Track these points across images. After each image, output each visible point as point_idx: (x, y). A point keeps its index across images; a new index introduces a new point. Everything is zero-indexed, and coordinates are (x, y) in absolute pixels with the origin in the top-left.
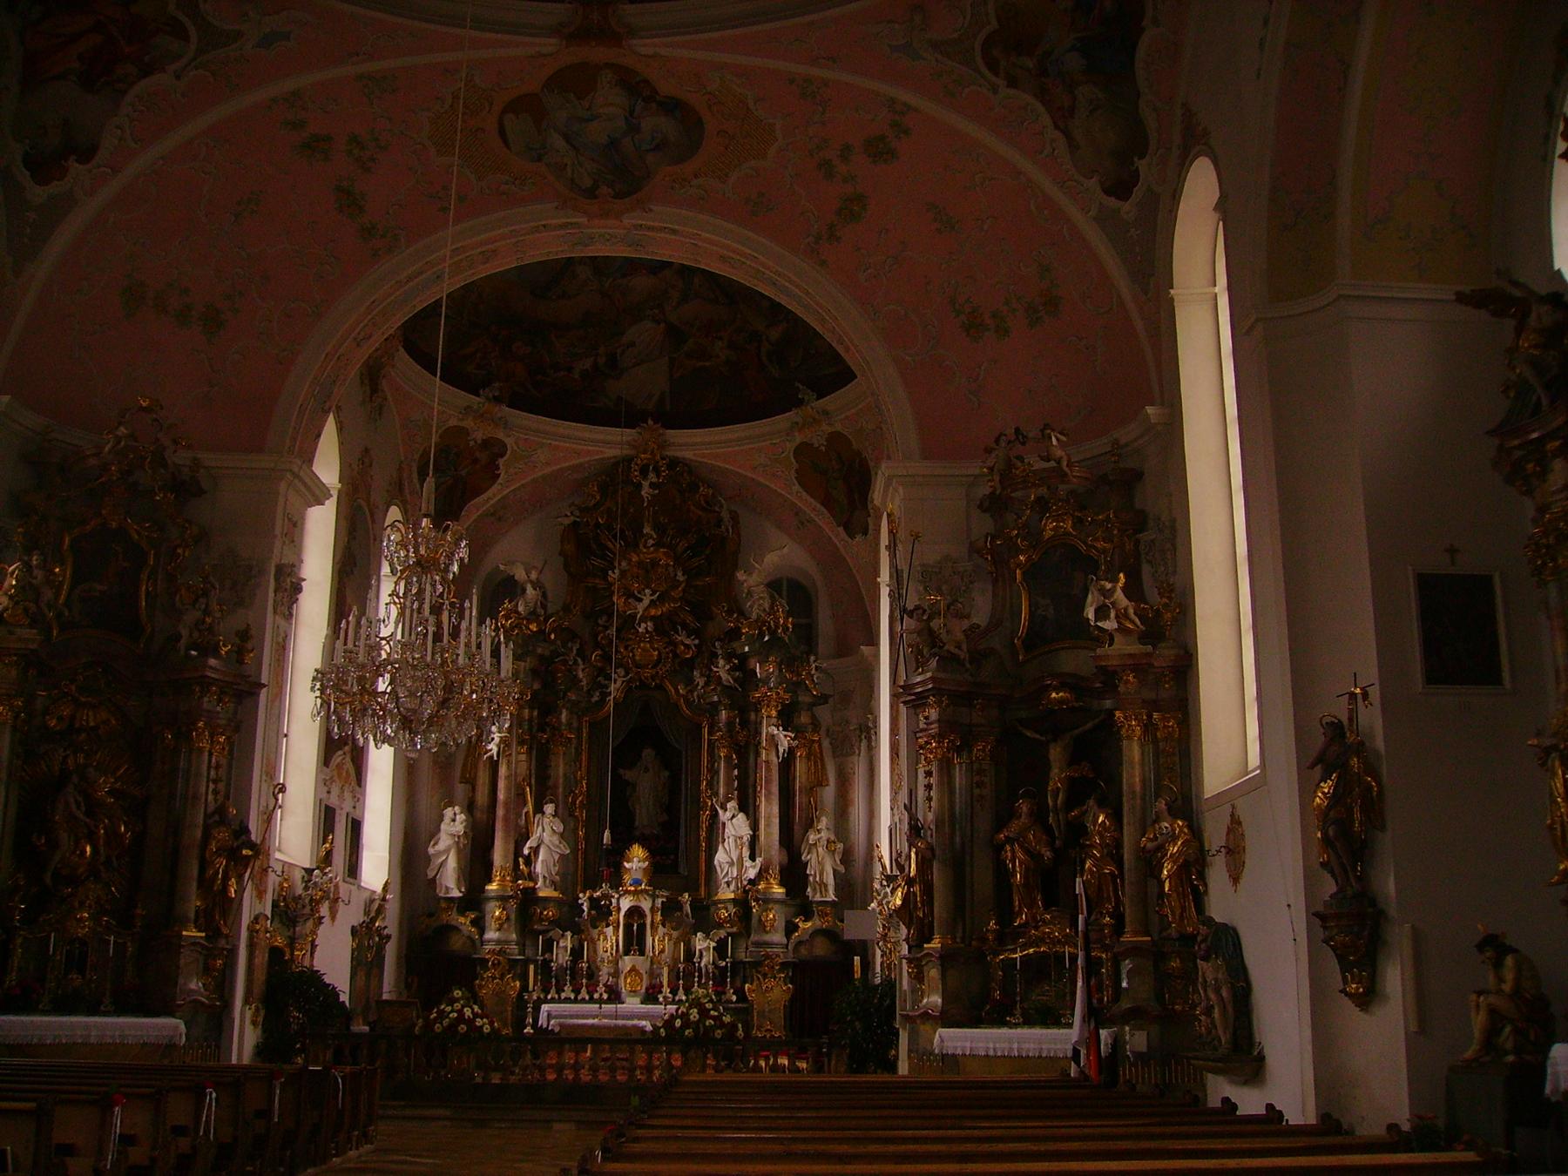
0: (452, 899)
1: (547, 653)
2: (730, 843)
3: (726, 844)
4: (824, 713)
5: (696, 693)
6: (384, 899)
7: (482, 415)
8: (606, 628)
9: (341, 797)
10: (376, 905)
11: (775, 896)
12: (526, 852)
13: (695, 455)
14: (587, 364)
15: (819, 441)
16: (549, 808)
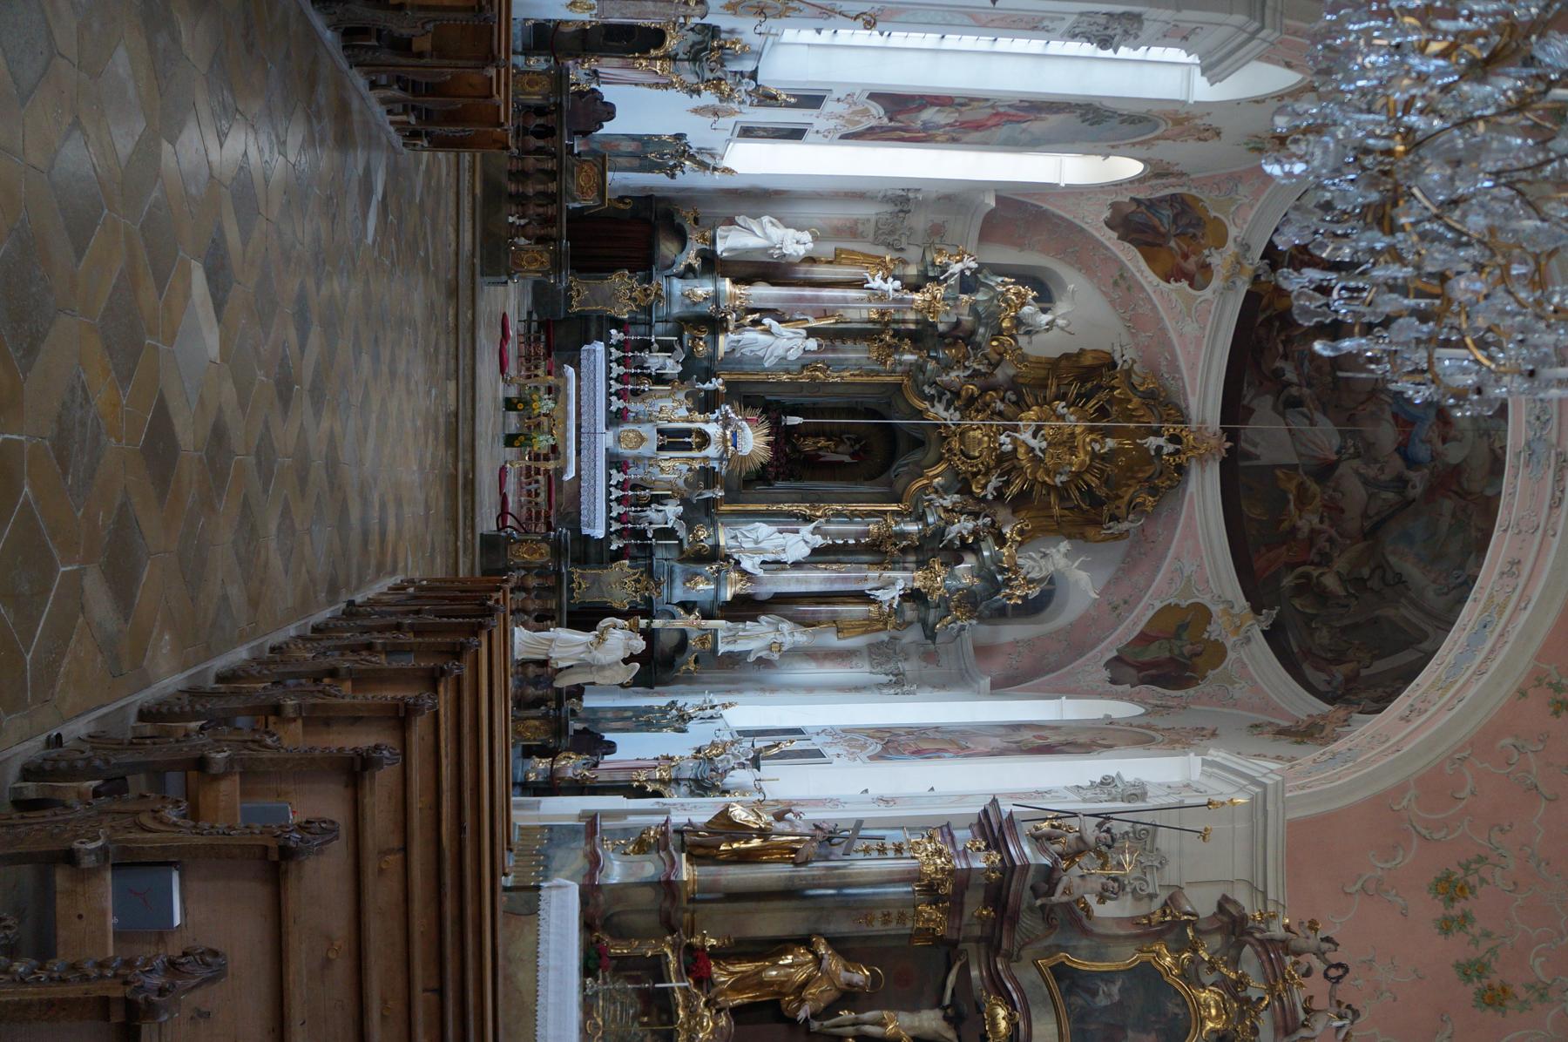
0: (714, 242)
1: (978, 338)
2: (779, 539)
3: (778, 535)
4: (913, 635)
5: (933, 496)
6: (715, 169)
7: (1238, 263)
8: (1002, 400)
9: (832, 116)
10: (708, 160)
11: (723, 590)
12: (767, 321)
13: (1192, 494)
14: (1291, 375)
15: (1214, 631)
16: (812, 344)
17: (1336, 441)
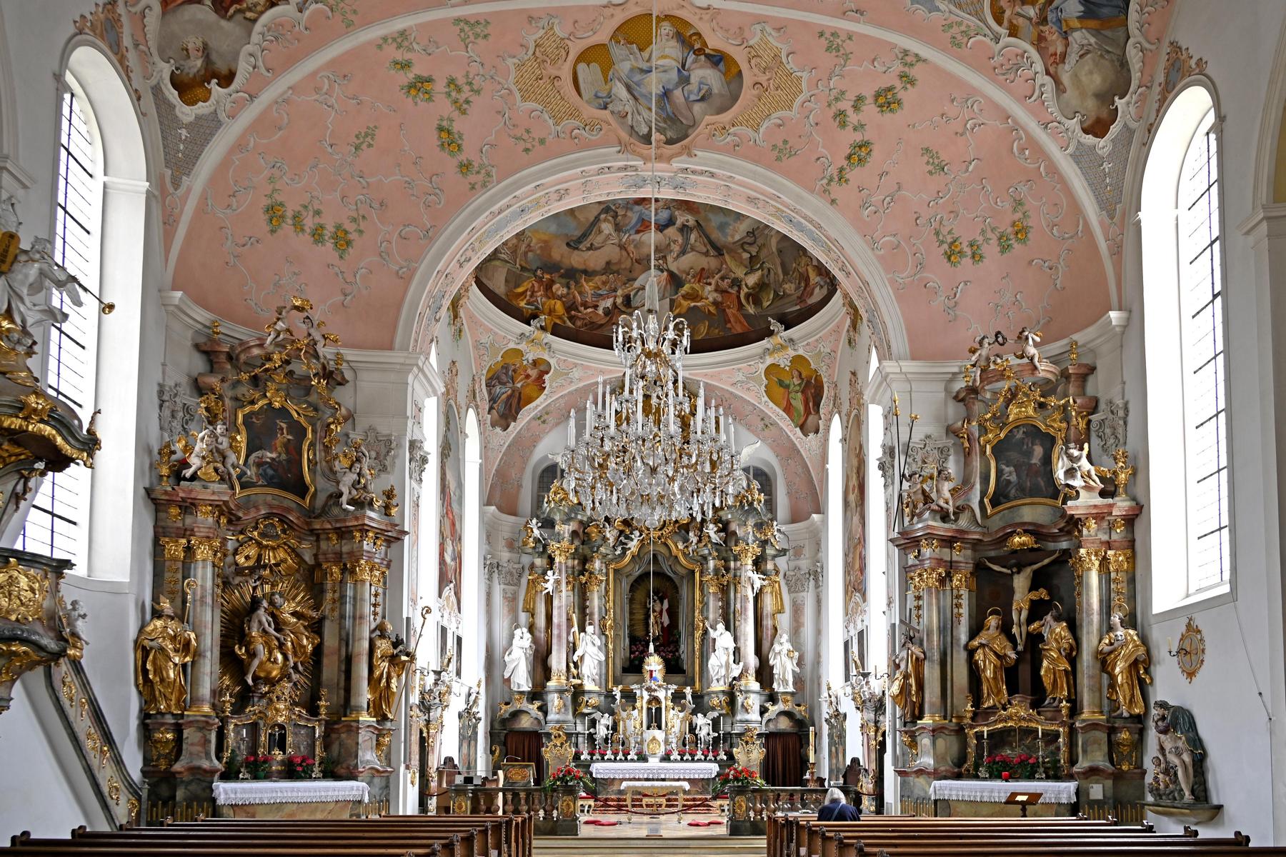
0: (522, 693)
10: (472, 698)
12: (575, 658)
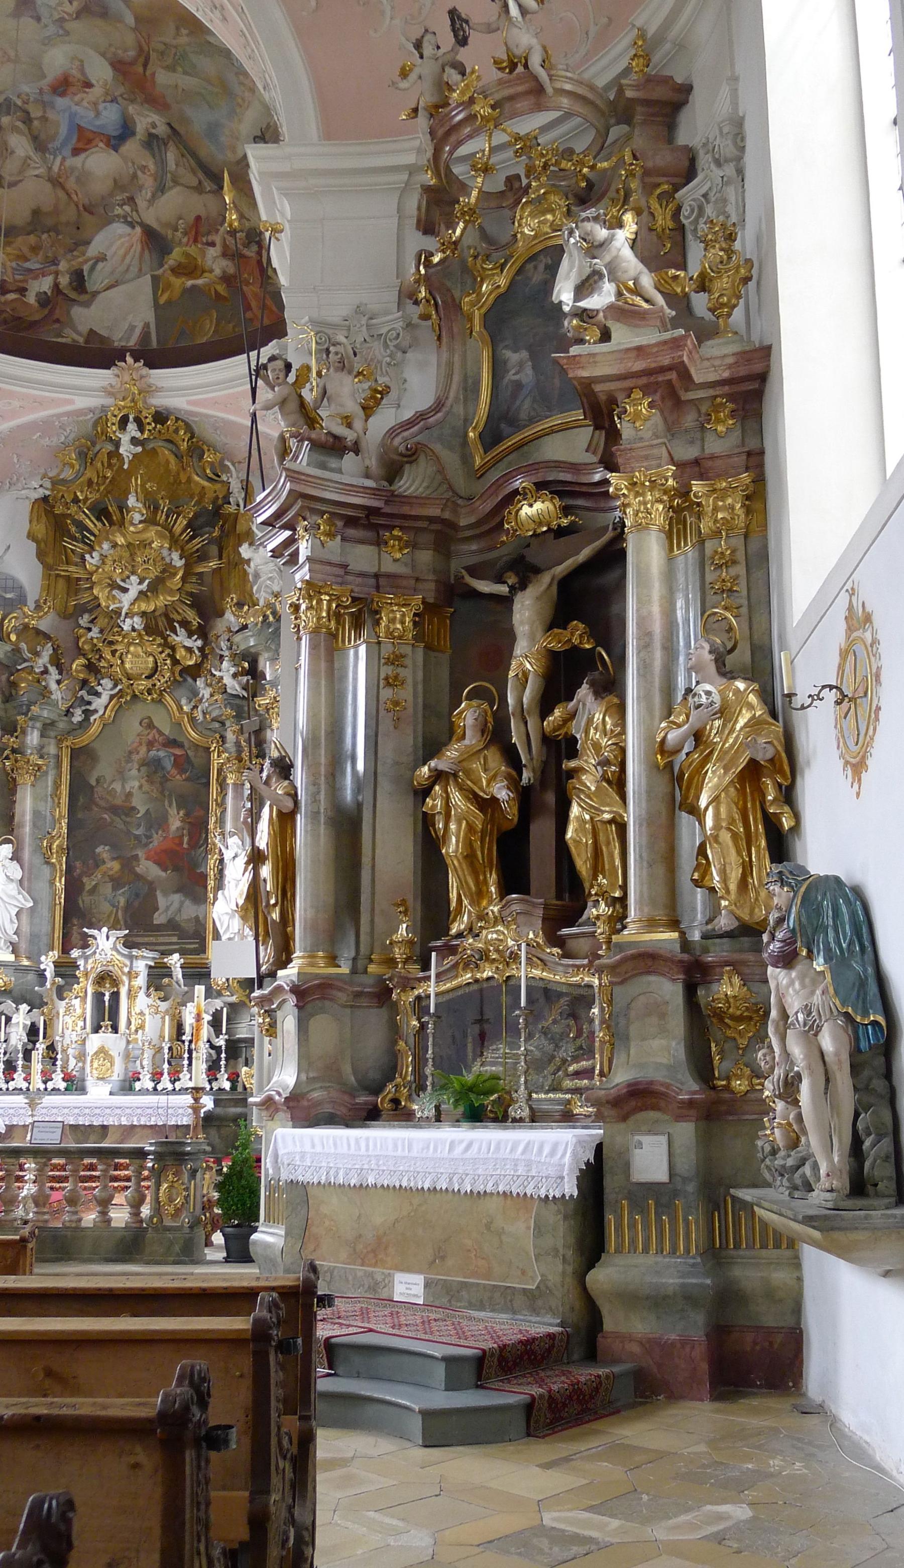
13: (189, 403)
14: (45, 285)
17: (119, 228)
